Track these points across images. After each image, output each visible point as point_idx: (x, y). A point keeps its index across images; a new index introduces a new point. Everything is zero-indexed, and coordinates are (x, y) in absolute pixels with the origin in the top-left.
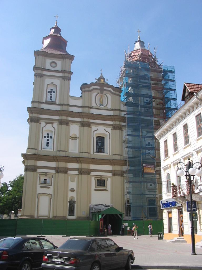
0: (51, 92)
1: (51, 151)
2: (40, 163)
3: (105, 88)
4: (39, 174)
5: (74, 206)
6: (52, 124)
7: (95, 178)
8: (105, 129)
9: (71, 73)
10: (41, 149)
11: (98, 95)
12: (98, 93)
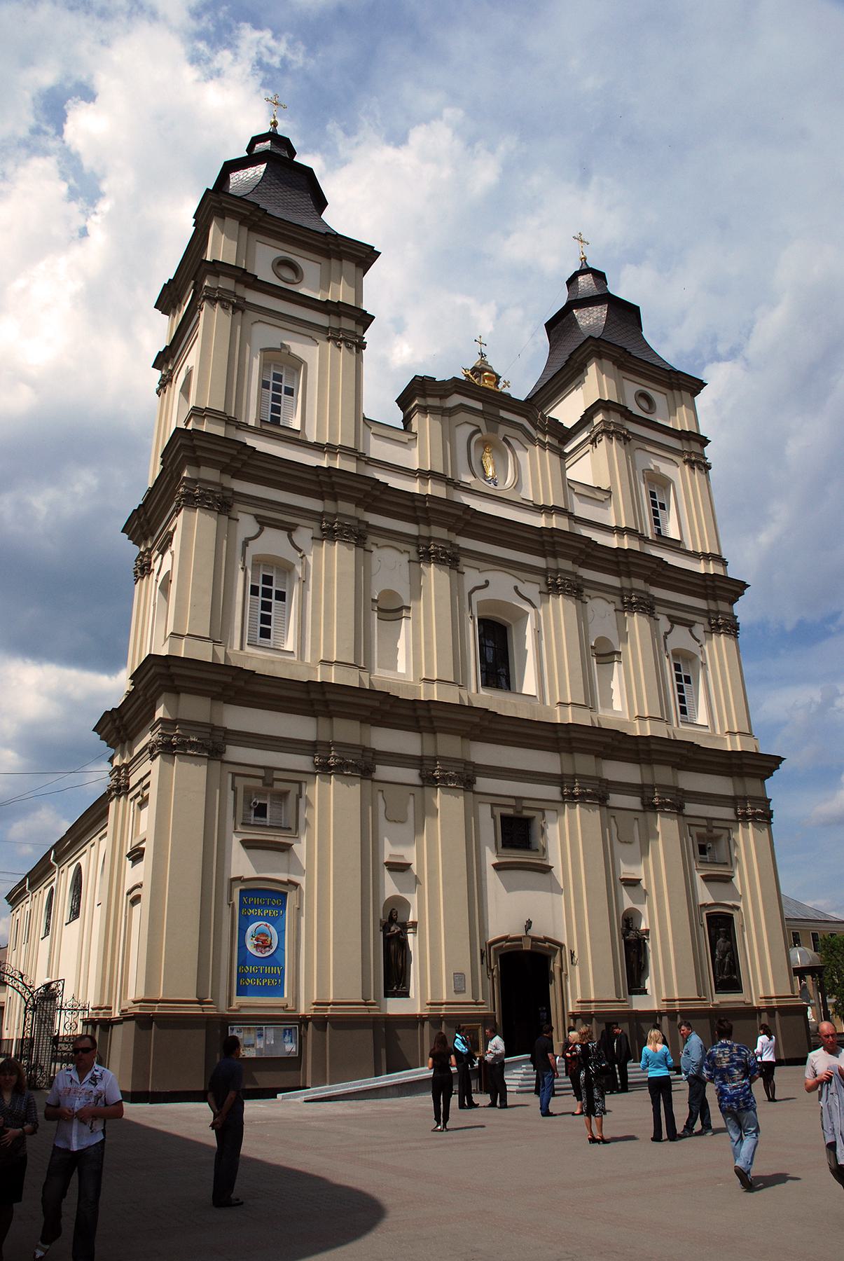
1: (290, 664)
2: (238, 718)
3: (503, 414)
4: (235, 775)
5: (404, 944)
6: (290, 529)
7: (493, 805)
8: (516, 588)
9: (365, 320)
11: (478, 436)
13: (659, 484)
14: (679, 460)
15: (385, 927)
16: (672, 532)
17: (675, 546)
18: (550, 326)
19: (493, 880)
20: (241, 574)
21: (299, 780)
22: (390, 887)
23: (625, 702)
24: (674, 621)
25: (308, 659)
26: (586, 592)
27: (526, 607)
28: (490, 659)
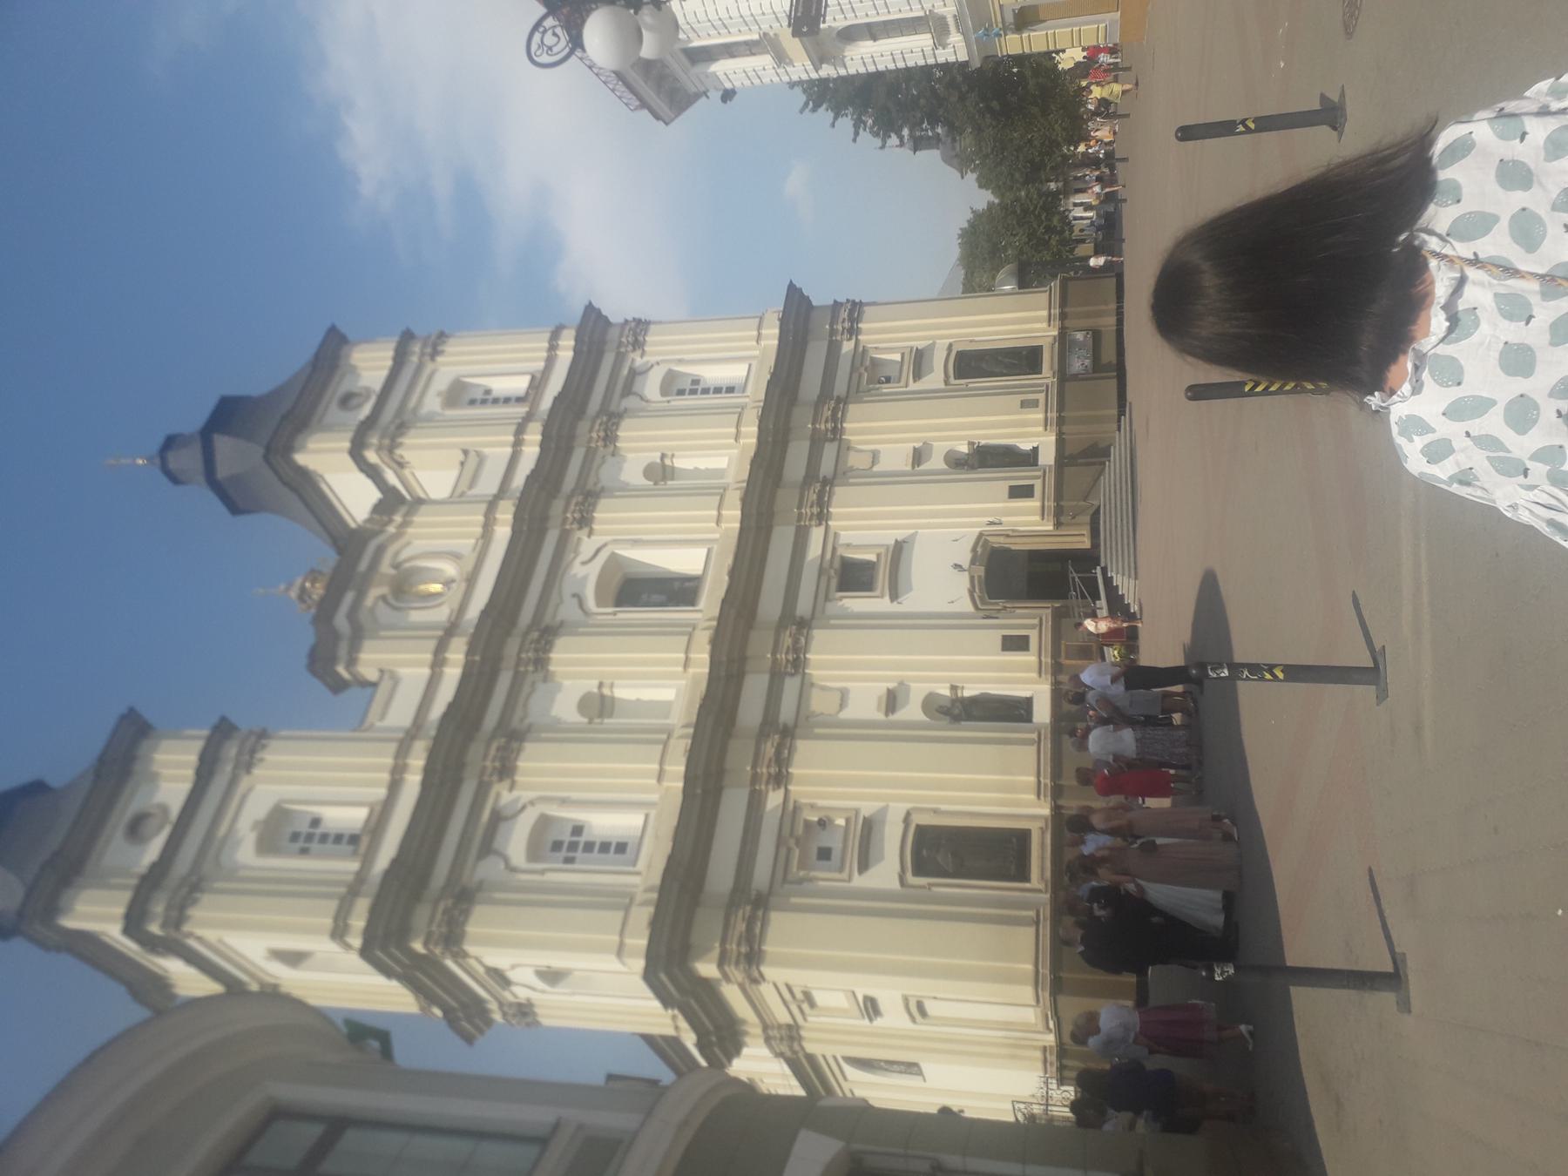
0: (309, 838)
3: (363, 566)
4: (785, 880)
6: (498, 818)
7: (827, 599)
8: (584, 563)
10: (638, 873)
12: (381, 603)
13: (458, 394)
14: (429, 367)
15: (956, 719)
16: (520, 384)
17: (538, 383)
18: (235, 509)
19: (910, 603)
20: (551, 877)
21: (791, 812)
22: (912, 711)
23: (720, 452)
24: (628, 390)
25: (654, 797)
26: (590, 485)
27: (603, 556)
28: (663, 598)
